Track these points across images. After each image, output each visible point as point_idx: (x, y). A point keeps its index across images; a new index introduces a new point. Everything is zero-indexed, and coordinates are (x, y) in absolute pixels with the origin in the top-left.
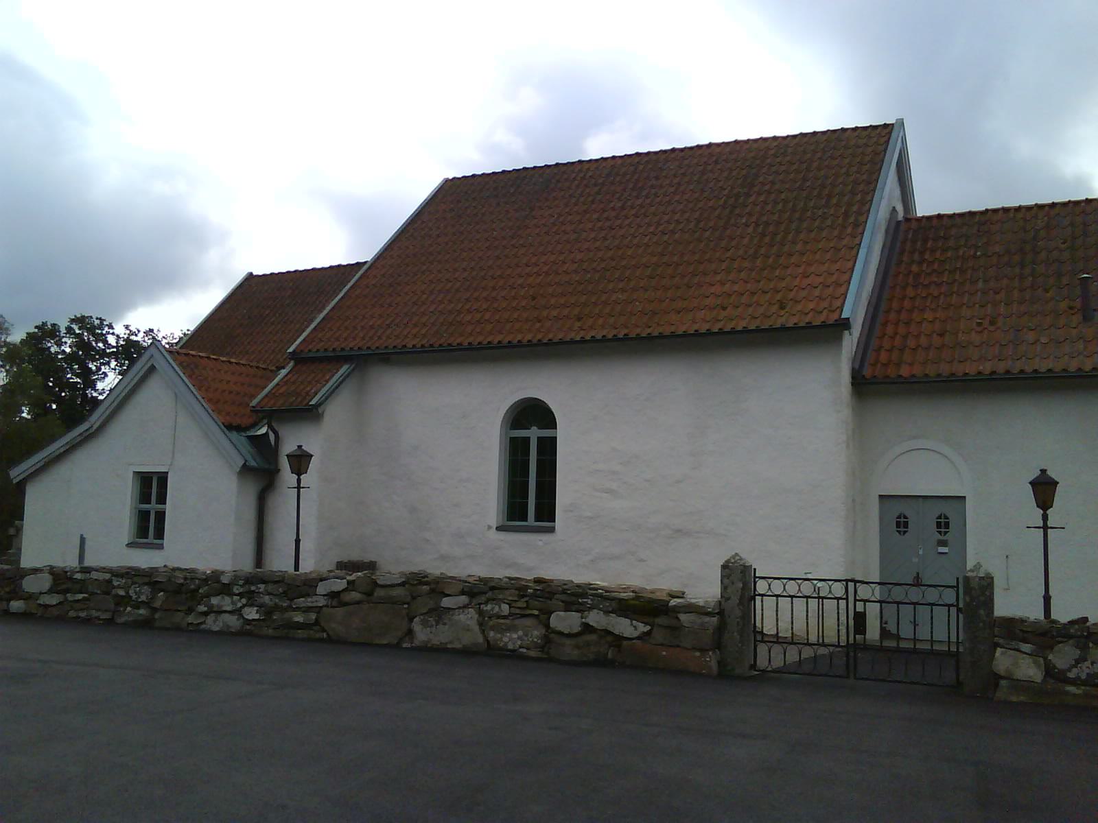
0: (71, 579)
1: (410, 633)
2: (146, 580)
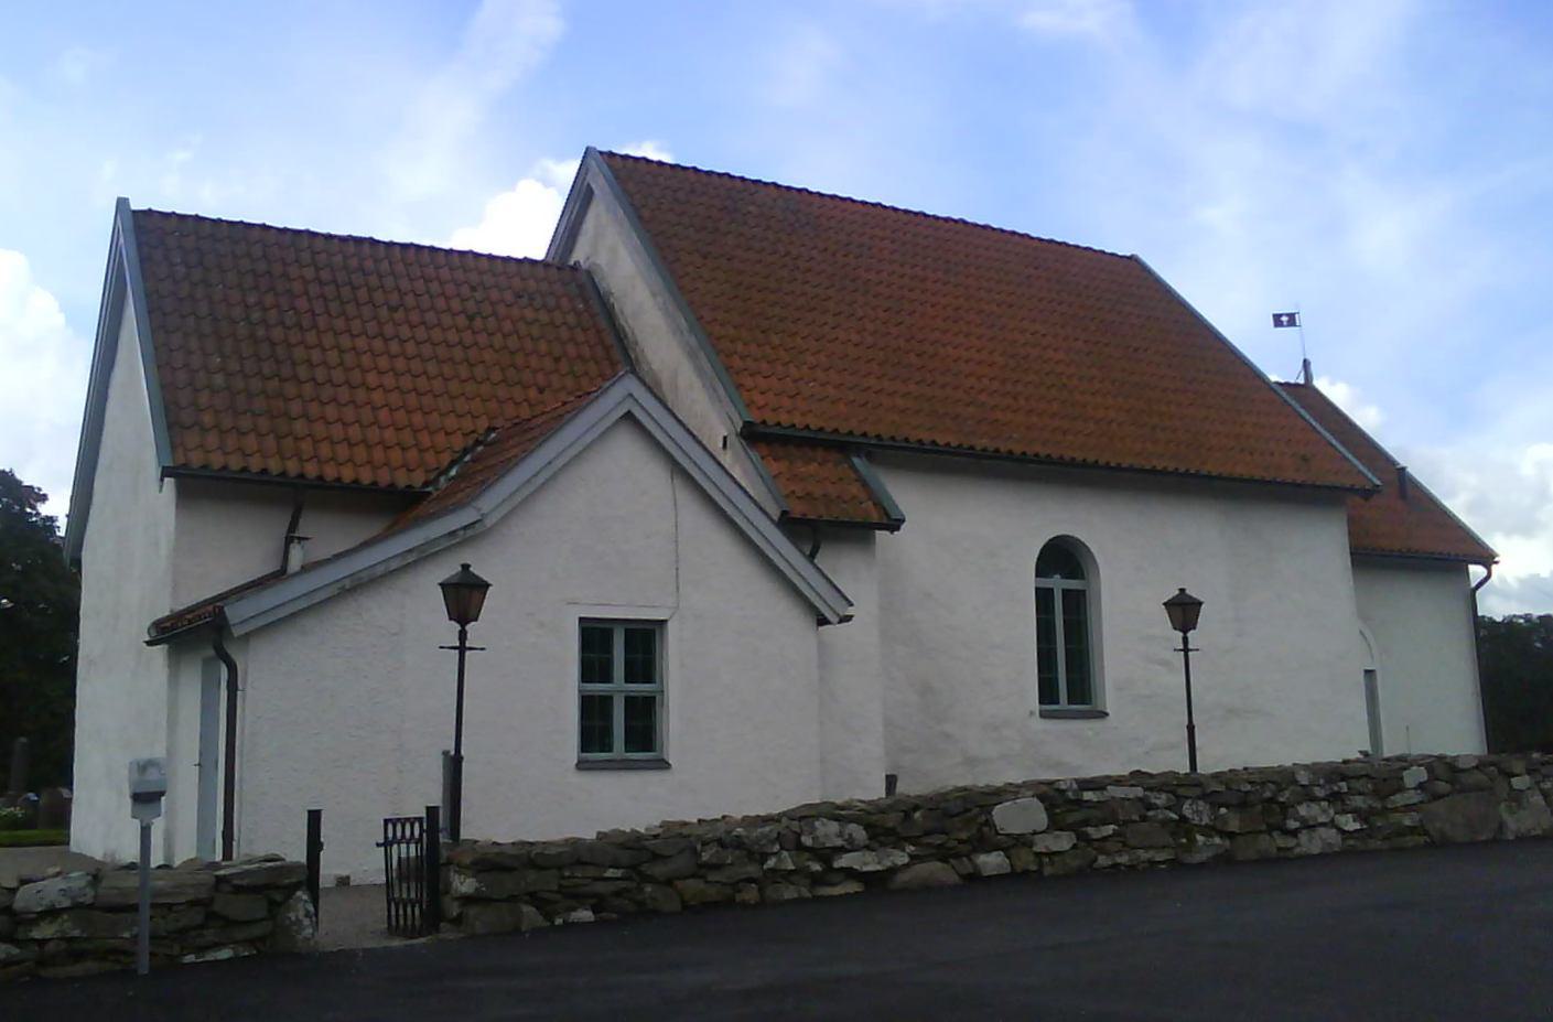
0: (1079, 803)
1: (1502, 826)
2: (1198, 791)
